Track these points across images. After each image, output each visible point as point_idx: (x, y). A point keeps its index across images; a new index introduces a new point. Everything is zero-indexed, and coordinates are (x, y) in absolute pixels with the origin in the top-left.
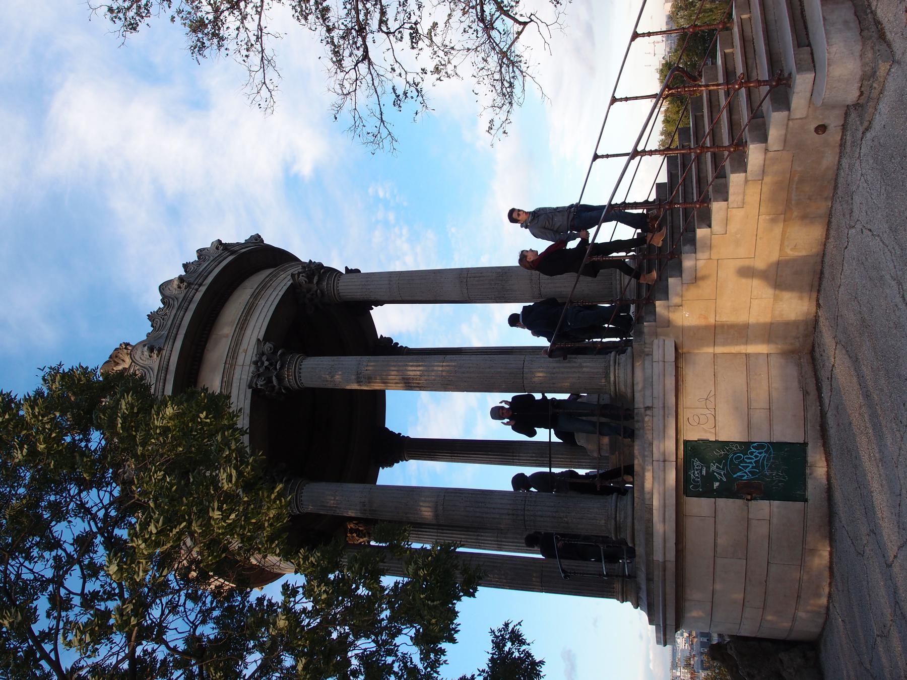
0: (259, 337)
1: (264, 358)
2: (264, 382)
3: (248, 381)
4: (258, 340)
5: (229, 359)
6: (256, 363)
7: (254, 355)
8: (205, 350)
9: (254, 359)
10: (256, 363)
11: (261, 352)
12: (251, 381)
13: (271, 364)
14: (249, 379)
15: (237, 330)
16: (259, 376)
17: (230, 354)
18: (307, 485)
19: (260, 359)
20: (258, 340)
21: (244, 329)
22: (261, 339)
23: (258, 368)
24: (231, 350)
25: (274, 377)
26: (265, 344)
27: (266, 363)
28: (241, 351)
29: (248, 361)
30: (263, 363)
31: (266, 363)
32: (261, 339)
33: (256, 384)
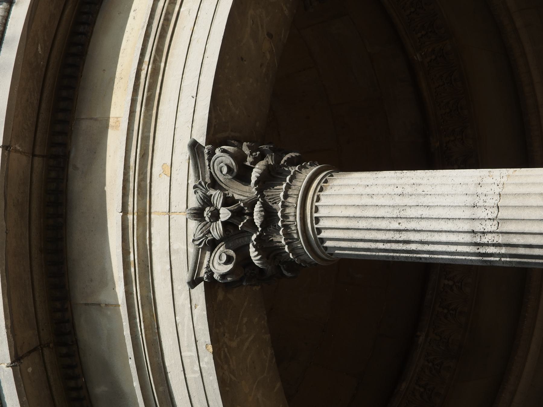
0: (195, 137)
2: (230, 267)
6: (198, 214)
7: (191, 191)
8: (71, 169)
9: (194, 202)
10: (198, 214)
12: (197, 265)
14: (192, 250)
16: (212, 245)
19: (207, 201)
20: (194, 146)
22: (202, 140)
25: (252, 249)
26: (212, 153)
28: (156, 170)
29: (179, 205)
30: (215, 216)
31: (225, 214)
32: (202, 140)
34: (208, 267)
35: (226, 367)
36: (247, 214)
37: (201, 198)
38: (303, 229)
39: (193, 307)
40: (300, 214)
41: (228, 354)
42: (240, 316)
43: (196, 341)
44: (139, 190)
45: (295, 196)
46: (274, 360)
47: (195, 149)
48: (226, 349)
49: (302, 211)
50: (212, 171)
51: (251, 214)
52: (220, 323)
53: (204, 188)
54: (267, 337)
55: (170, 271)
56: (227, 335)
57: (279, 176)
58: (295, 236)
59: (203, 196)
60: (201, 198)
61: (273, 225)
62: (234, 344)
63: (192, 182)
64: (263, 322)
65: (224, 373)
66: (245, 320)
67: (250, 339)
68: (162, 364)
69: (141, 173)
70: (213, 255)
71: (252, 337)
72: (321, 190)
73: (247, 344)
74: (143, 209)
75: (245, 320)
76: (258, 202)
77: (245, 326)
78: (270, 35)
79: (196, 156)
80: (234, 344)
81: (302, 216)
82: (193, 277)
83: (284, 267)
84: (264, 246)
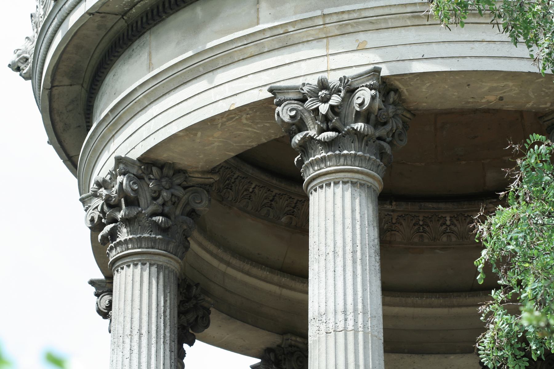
1: (335, 100)
3: (278, 84)
4: (377, 71)
5: (335, 18)
6: (323, 85)
10: (323, 85)
11: (355, 85)
13: (326, 118)
15: (409, 9)
17: (346, 17)
18: (154, 269)
20: (377, 71)
21: (417, 22)
23: (314, 93)
24: (355, 15)
27: (324, 108)
28: (362, 37)
33: (279, 104)
34: (285, 100)
35: (224, 120)
36: (328, 126)
37: (335, 86)
38: (321, 174)
39: (260, 89)
40: (331, 170)
41: (234, 119)
42: (268, 121)
43: (236, 95)
44: (344, 25)
45: (345, 163)
46: (249, 148)
47: (372, 73)
48: (237, 117)
49: (333, 172)
50: (360, 89)
51: (328, 130)
52: (255, 110)
53: (345, 85)
54: (264, 140)
55: (285, 63)
56: (248, 116)
57: (363, 144)
58: (316, 168)
59: (336, 88)
60: (335, 86)
61: (322, 148)
62: (245, 121)
63: (350, 73)
64: (273, 136)
65: (219, 119)
66: (268, 125)
67: (255, 130)
68: (219, 67)
69: (357, 24)
70: (296, 102)
71: (258, 131)
72: (353, 184)
73: (250, 129)
74: (329, 31)
75: (268, 125)
76: (337, 133)
77: (262, 125)
78: (501, 99)
79: (368, 74)
80: (245, 121)
81: (330, 172)
82: (275, 90)
83: (299, 158)
84: (307, 143)
